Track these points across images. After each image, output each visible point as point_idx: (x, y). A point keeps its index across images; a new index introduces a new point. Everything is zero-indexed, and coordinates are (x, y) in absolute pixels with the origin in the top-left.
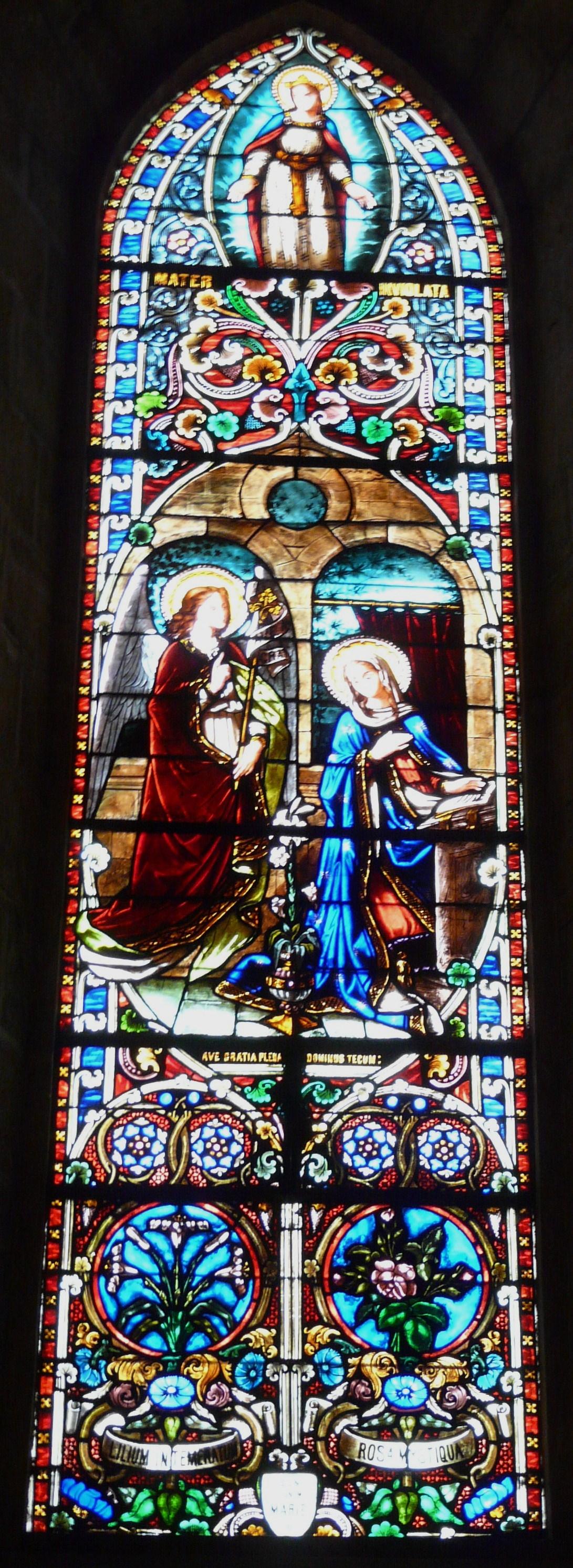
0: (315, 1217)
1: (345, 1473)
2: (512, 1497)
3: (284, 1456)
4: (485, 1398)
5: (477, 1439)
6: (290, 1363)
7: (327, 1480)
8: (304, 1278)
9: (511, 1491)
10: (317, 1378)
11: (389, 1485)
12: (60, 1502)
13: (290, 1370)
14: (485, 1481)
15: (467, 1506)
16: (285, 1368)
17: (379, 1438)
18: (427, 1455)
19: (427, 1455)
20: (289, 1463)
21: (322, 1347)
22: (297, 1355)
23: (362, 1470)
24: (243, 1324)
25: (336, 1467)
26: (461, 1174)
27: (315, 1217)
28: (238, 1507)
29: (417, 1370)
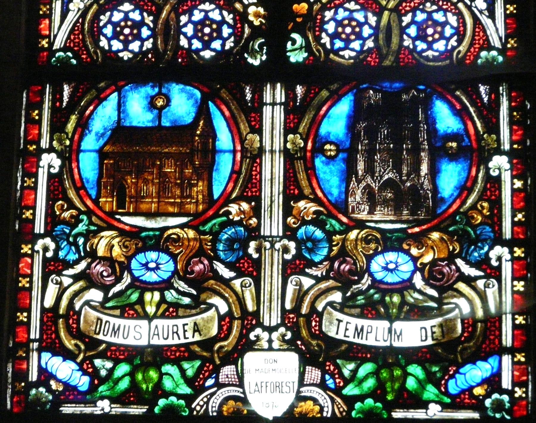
3: (265, 336)
7: (308, 359)
18: (413, 334)
20: (270, 341)
23: (343, 348)
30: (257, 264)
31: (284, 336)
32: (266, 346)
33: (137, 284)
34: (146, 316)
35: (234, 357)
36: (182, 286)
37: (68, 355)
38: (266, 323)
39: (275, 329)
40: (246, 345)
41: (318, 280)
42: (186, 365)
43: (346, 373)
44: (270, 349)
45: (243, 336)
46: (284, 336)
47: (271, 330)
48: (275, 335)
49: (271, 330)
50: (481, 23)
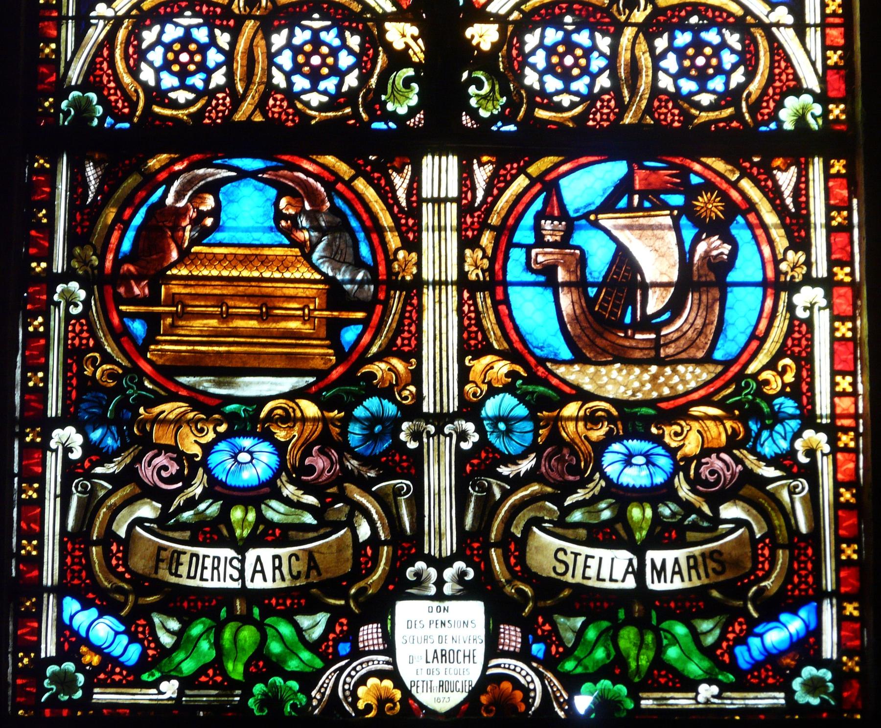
0: (482, 175)
1: (536, 598)
2: (814, 633)
4: (770, 472)
5: (754, 542)
6: (440, 419)
8: (463, 282)
9: (813, 625)
10: (483, 444)
11: (611, 616)
12: (59, 646)
13: (440, 431)
14: (772, 608)
15: (740, 650)
16: (432, 429)
17: (591, 542)
19: (671, 569)
21: (493, 391)
22: (453, 406)
24: (355, 356)
25: (519, 591)
26: (731, 97)
27: (482, 175)
28: (356, 653)
29: (654, 430)
30: (417, 457)
31: (463, 574)
32: (433, 591)
33: (216, 489)
34: (230, 541)
35: (380, 609)
36: (289, 490)
37: (108, 608)
38: (435, 552)
39: (448, 562)
40: (399, 587)
41: (518, 482)
42: (305, 621)
43: (569, 637)
44: (440, 596)
45: (396, 574)
46: (463, 574)
47: (441, 564)
48: (449, 574)
49: (441, 564)
50: (781, 46)
